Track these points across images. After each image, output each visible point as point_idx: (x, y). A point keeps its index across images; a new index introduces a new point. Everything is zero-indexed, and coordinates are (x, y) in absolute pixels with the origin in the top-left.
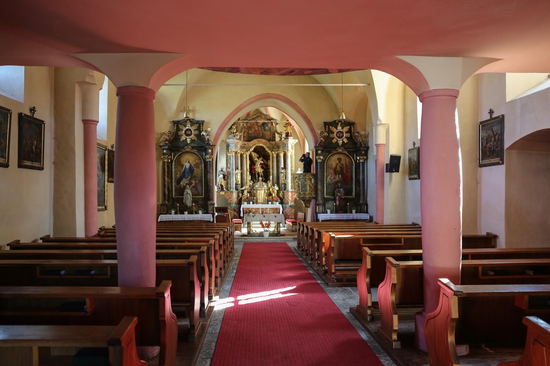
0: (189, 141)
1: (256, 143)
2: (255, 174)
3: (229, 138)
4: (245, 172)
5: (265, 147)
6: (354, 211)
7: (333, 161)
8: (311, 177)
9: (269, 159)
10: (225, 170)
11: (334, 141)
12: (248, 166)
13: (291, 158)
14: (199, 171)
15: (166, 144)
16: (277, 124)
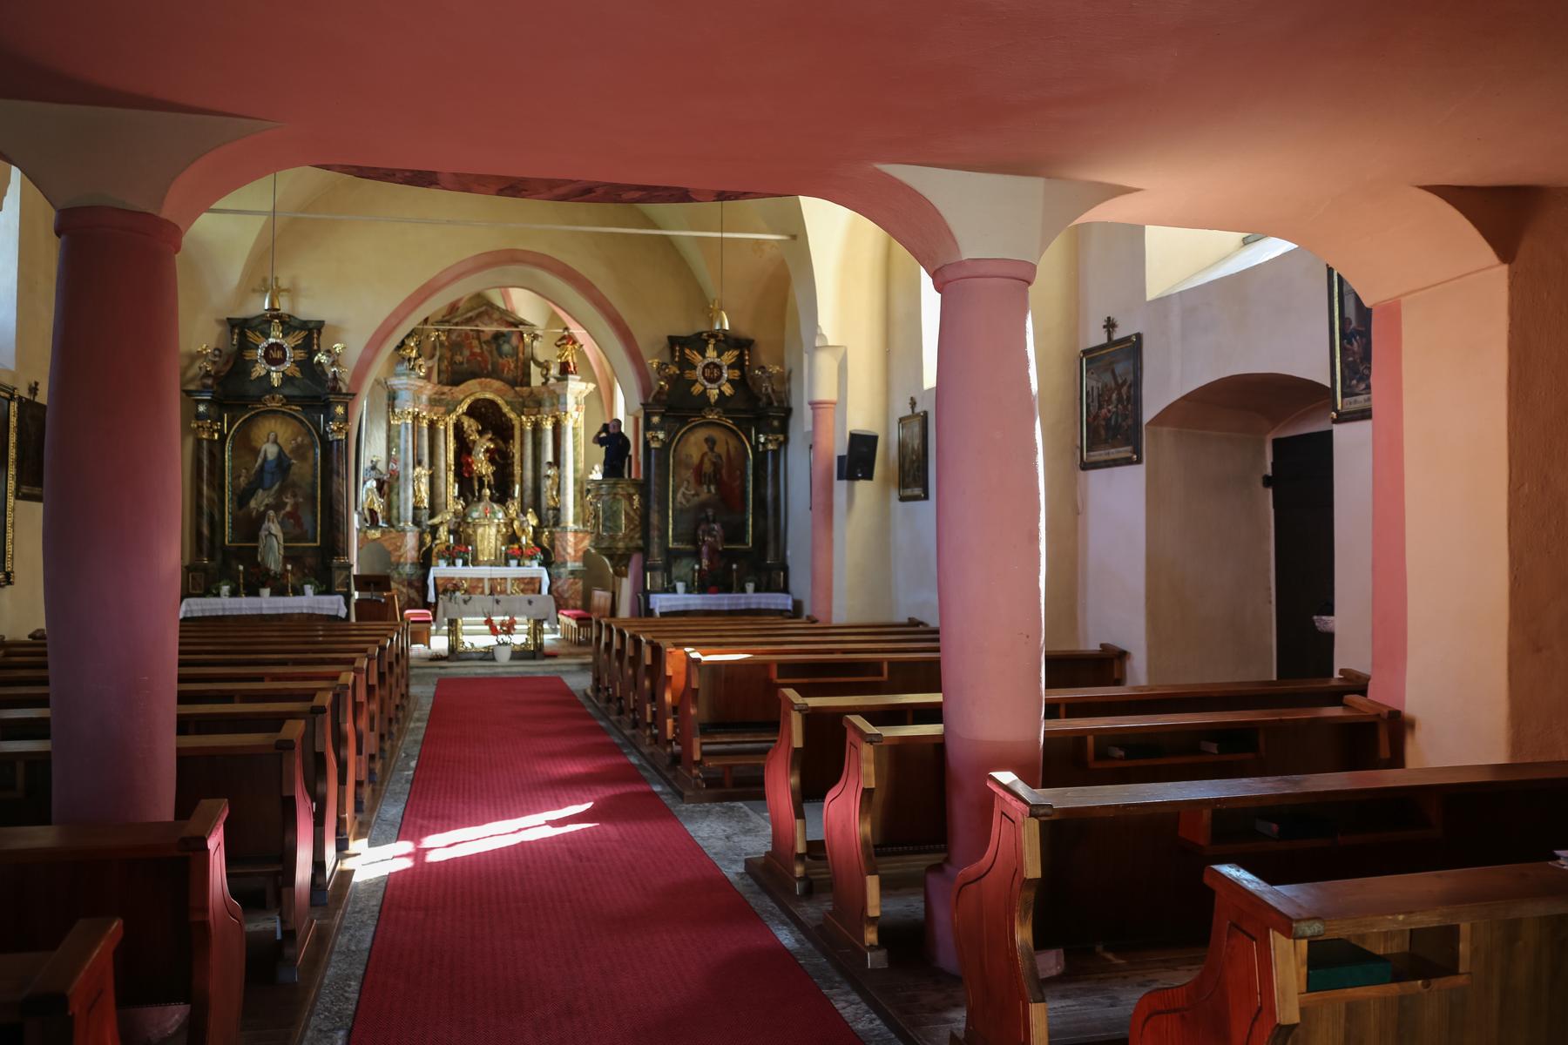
0: (276, 378)
2: (471, 479)
3: (397, 375)
4: (443, 474)
5: (500, 401)
6: (750, 587)
7: (694, 445)
8: (632, 491)
9: (512, 437)
10: (382, 466)
11: (697, 389)
12: (451, 456)
13: (575, 436)
14: (305, 470)
15: (205, 386)
16: (535, 337)
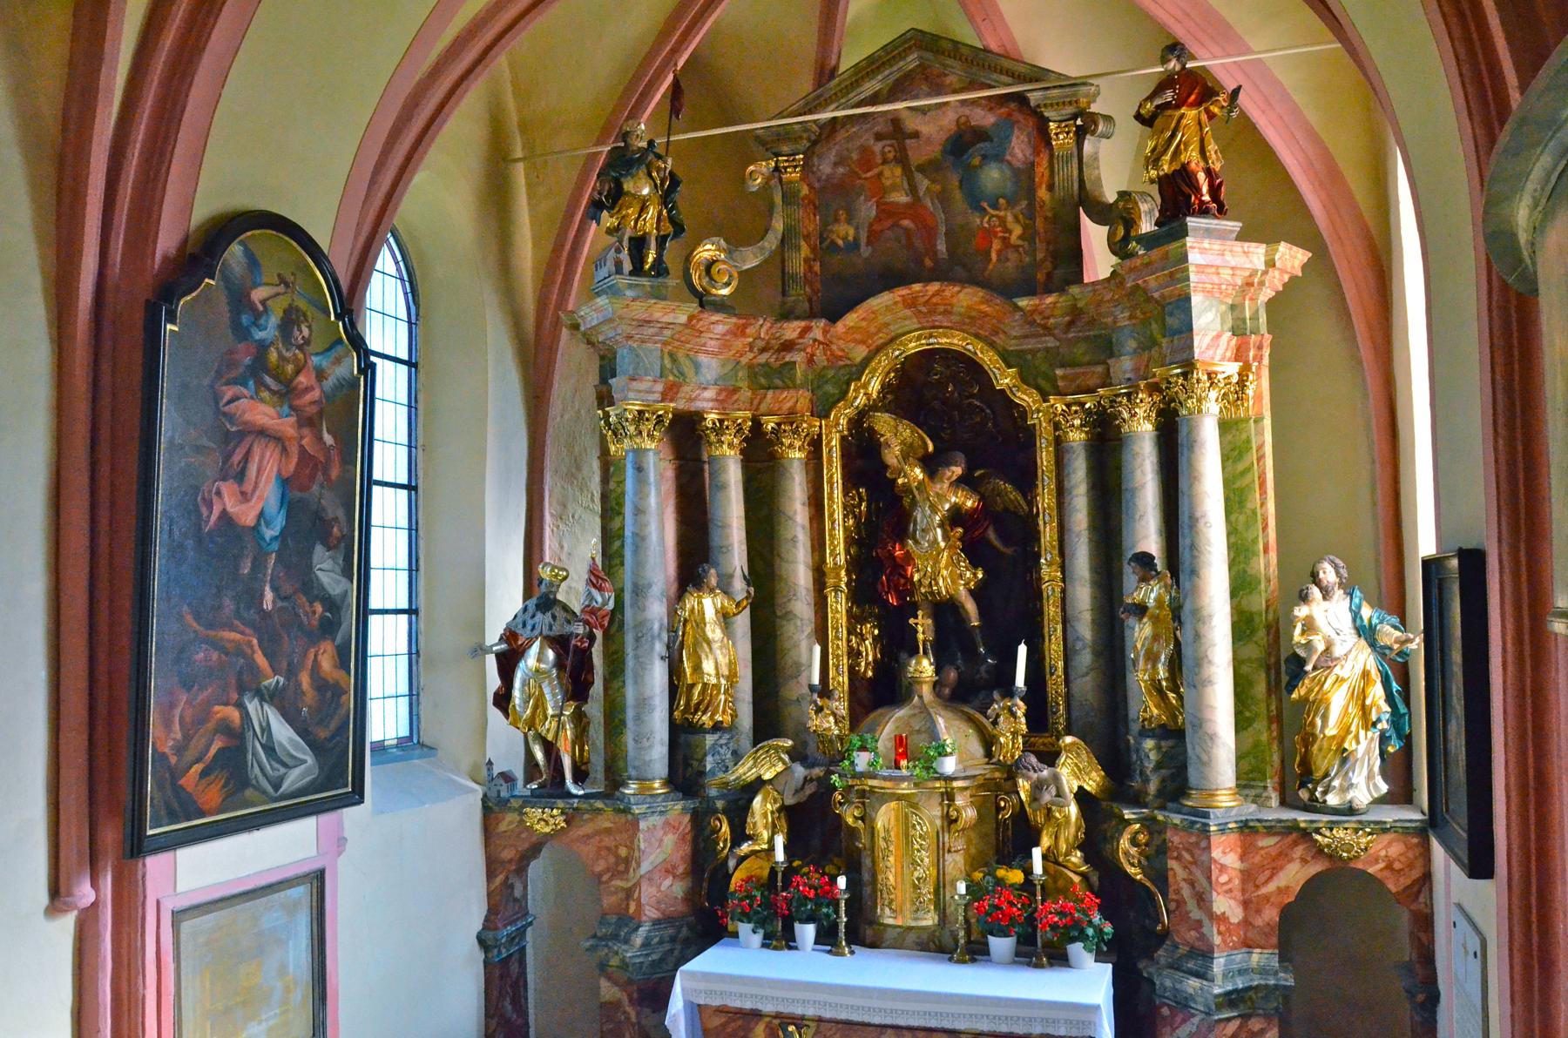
1: (897, 327)
5: (988, 358)
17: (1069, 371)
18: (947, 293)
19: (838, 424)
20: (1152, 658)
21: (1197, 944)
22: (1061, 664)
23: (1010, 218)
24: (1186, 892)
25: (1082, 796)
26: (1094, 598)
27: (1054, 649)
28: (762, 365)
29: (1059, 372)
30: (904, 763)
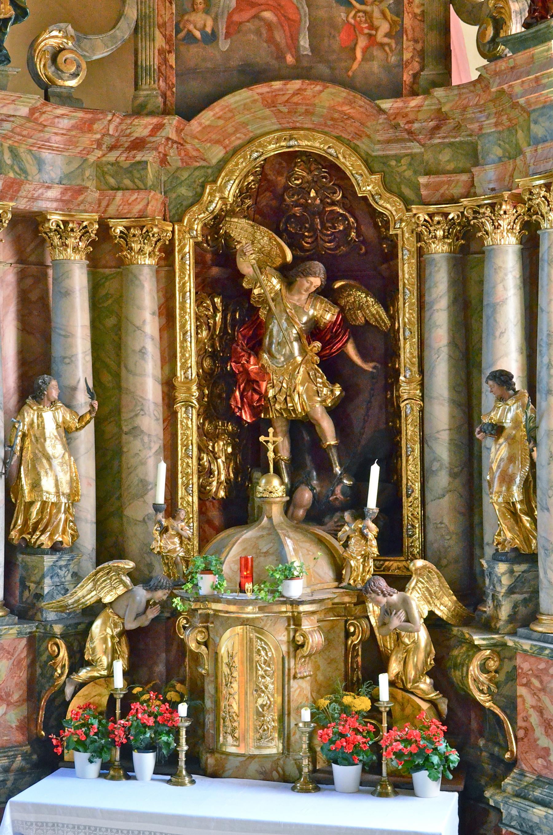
5: (350, 163)
17: (433, 179)
18: (309, 93)
19: (191, 229)
20: (507, 479)
21: (544, 772)
22: (417, 486)
23: (377, 14)
24: (534, 719)
25: (433, 622)
26: (452, 417)
27: (410, 470)
28: (112, 165)
29: (423, 180)
30: (248, 586)
